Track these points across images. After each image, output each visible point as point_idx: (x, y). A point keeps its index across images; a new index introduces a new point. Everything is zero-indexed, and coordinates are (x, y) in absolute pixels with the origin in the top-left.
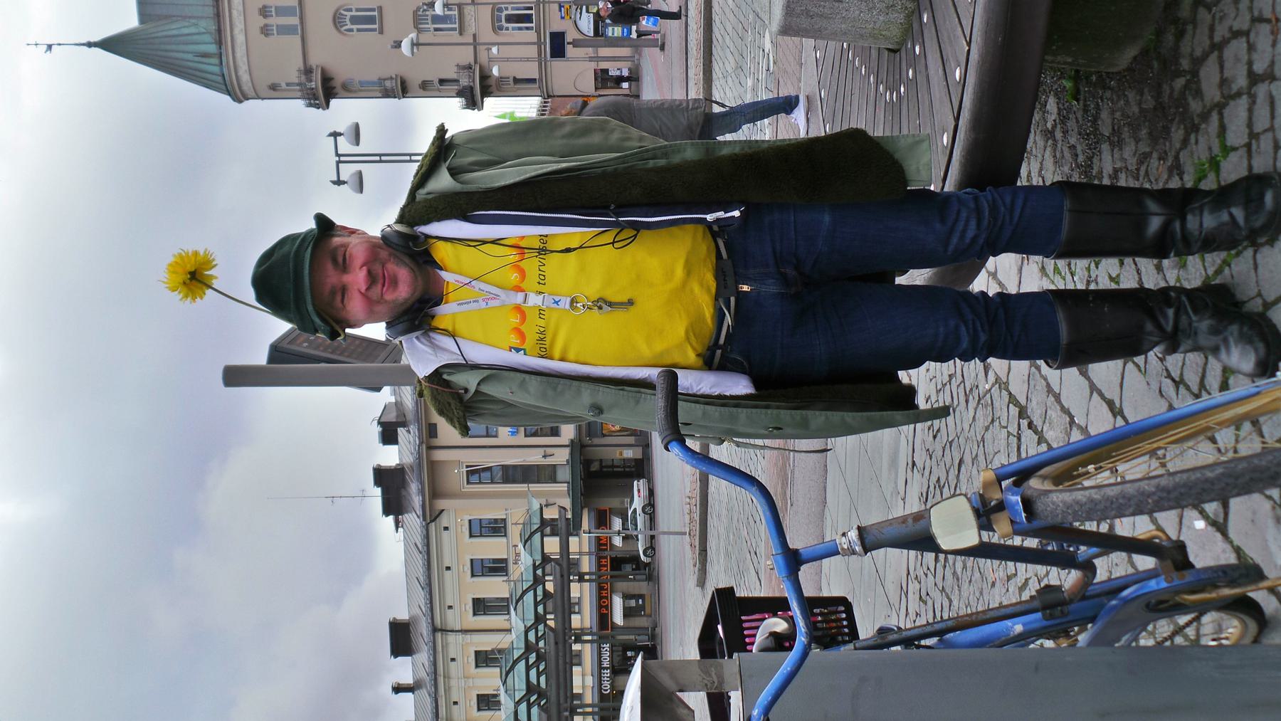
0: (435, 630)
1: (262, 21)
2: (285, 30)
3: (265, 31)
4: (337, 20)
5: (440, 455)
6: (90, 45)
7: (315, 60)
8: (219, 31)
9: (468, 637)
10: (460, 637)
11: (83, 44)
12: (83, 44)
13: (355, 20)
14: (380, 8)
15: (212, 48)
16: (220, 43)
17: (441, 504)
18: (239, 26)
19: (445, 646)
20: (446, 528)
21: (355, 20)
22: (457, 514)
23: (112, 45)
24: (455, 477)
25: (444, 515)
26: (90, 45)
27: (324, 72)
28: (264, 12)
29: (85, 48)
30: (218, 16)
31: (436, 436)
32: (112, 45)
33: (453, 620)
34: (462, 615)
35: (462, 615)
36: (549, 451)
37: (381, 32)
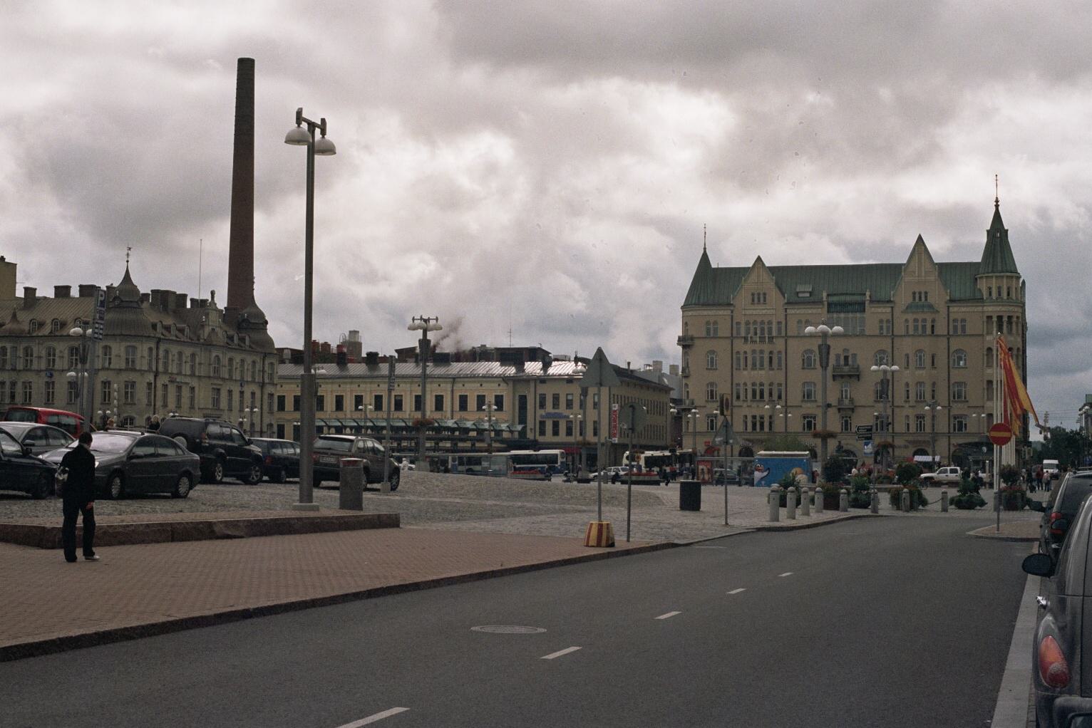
0: (454, 379)
2: (708, 331)
3: (708, 323)
4: (713, 352)
5: (532, 384)
6: (705, 249)
7: (697, 342)
8: (709, 305)
9: (449, 393)
10: (450, 389)
11: (705, 245)
12: (705, 245)
13: (712, 359)
14: (716, 369)
15: (701, 301)
16: (703, 305)
17: (511, 384)
18: (710, 313)
19: (446, 383)
20: (499, 385)
21: (712, 359)
22: (504, 390)
23: (705, 258)
24: (522, 391)
25: (505, 385)
26: (705, 249)
27: (692, 345)
28: (715, 323)
29: (703, 247)
30: (714, 305)
32: (705, 258)
33: (458, 386)
34: (460, 390)
35: (460, 390)
36: (533, 431)
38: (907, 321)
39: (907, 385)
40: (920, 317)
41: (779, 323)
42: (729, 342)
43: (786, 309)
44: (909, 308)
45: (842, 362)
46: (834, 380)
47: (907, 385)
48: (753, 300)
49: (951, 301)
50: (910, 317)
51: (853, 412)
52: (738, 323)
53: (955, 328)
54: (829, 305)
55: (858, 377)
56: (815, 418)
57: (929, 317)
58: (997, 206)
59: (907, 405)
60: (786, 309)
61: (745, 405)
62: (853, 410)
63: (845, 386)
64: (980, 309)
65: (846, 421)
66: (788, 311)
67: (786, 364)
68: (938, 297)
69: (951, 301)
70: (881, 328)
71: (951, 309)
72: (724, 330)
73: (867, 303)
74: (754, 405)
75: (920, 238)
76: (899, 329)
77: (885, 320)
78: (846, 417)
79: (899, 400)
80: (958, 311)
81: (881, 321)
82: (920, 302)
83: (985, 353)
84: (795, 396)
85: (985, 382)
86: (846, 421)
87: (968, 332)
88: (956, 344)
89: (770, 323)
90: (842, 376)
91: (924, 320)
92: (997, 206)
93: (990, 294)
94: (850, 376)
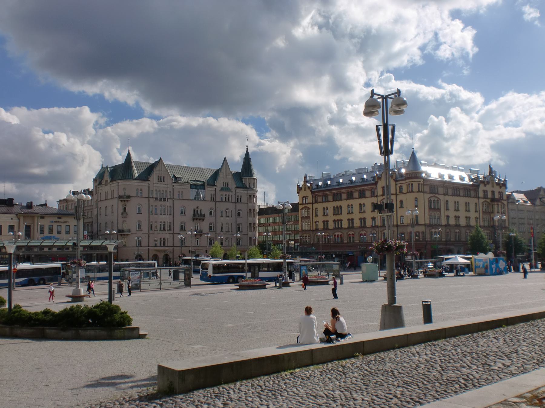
1: (139, 189)
4: (139, 204)
31: (41, 218)
37: (137, 213)
38: (221, 195)
39: (222, 224)
40: (227, 193)
41: (170, 192)
42: (147, 199)
43: (173, 185)
44: (222, 189)
45: (196, 213)
46: (193, 221)
47: (222, 224)
48: (158, 180)
49: (237, 187)
50: (224, 193)
51: (201, 236)
52: (152, 191)
53: (238, 199)
54: (191, 185)
55: (203, 220)
56: (213, 239)
57: (230, 194)
58: (247, 148)
59: (222, 233)
60: (173, 185)
61: (156, 232)
62: (201, 235)
63: (197, 224)
64: (246, 192)
65: (197, 240)
66: (174, 186)
67: (173, 212)
68: (232, 185)
69: (237, 187)
70: (211, 198)
71: (237, 191)
72: (145, 194)
73: (206, 185)
74: (161, 232)
75: (225, 158)
76: (218, 199)
77: (213, 194)
78: (197, 239)
79: (219, 231)
80: (240, 192)
81: (211, 195)
82: (225, 188)
83: (248, 211)
84: (177, 229)
85: (248, 224)
86: (197, 240)
87: (242, 201)
88: (239, 206)
89: (166, 191)
90: (197, 219)
91: (229, 196)
92: (247, 148)
93: (250, 186)
94: (200, 219)
